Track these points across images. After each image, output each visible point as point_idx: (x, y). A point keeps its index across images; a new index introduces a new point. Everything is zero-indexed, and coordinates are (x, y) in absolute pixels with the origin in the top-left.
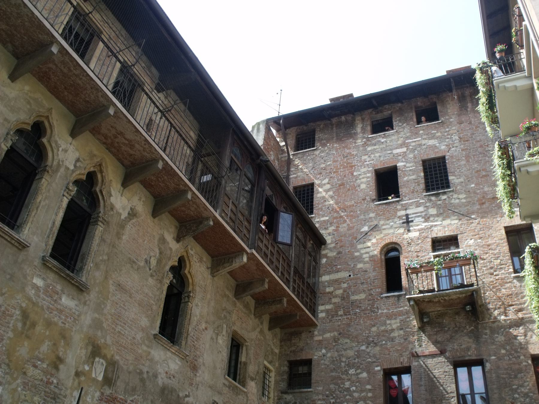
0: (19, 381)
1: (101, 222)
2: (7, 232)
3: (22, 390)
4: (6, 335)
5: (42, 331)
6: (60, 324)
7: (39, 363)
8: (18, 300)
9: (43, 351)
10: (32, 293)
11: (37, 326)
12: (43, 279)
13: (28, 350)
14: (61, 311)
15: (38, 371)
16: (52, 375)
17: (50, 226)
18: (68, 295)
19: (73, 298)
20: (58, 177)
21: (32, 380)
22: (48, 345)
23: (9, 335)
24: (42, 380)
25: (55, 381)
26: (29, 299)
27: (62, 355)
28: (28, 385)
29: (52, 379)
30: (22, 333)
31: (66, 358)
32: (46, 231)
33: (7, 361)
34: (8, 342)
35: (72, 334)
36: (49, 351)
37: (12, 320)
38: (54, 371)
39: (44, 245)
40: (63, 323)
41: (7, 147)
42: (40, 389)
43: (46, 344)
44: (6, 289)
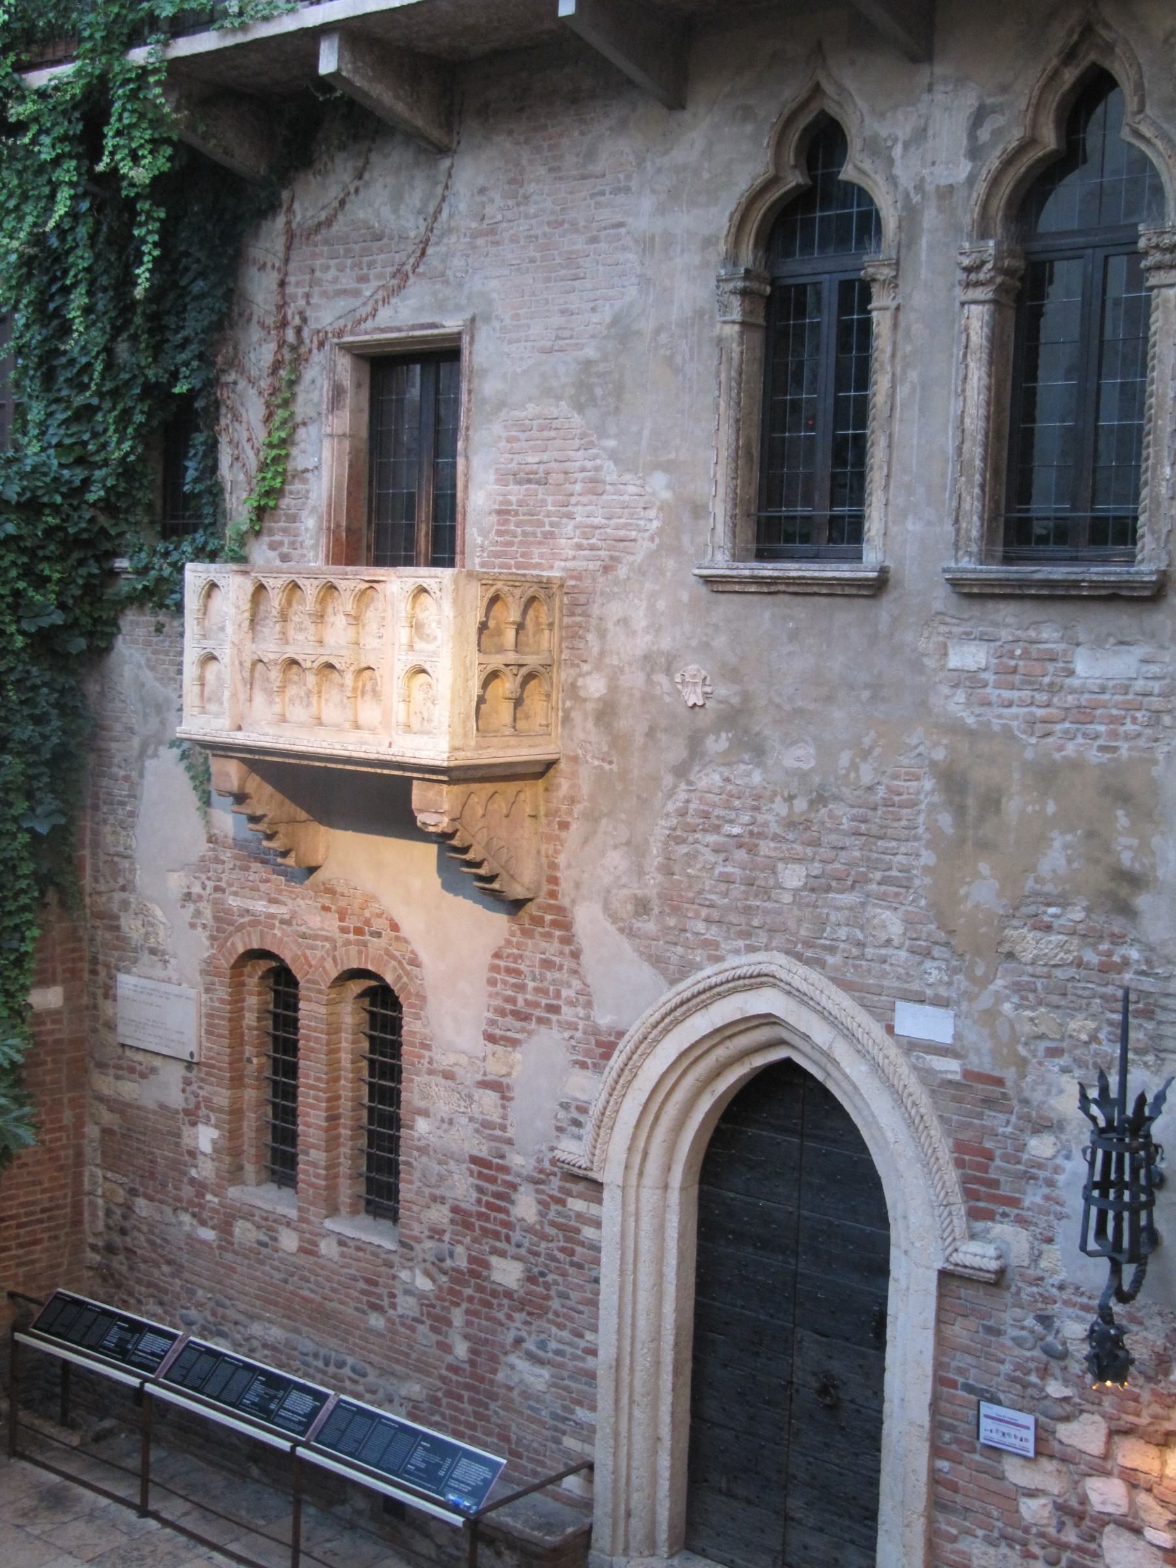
0: (999, 983)
1: (1158, 267)
2: (799, 578)
3: (1018, 1007)
4: (915, 863)
5: (1030, 809)
6: (1094, 756)
7: (1052, 910)
8: (916, 747)
9: (1054, 871)
10: (956, 704)
11: (1004, 800)
12: (984, 639)
13: (997, 885)
14: (1084, 715)
15: (1055, 938)
16: (1118, 940)
17: (951, 450)
18: (1098, 643)
19: (1122, 643)
20: (923, 256)
21: (1039, 970)
22: (1066, 847)
23: (923, 861)
24: (1079, 964)
25: (1134, 954)
26: (956, 728)
27: (1133, 859)
28: (1035, 991)
29: (1123, 950)
30: (963, 841)
31: (1153, 867)
32: (944, 475)
33: (942, 936)
34: (928, 880)
35: (1156, 771)
36: (1075, 865)
37: (919, 813)
38: (1118, 925)
39: (949, 528)
40: (1102, 749)
41: (733, 322)
42: (1080, 992)
43: (1057, 844)
44: (873, 734)
